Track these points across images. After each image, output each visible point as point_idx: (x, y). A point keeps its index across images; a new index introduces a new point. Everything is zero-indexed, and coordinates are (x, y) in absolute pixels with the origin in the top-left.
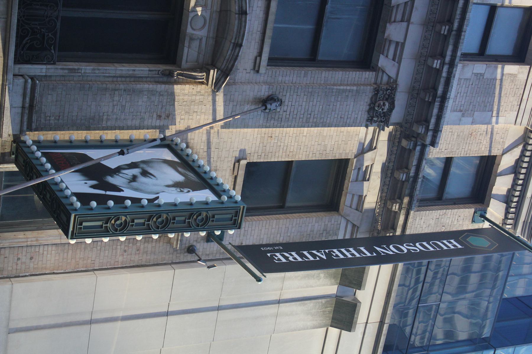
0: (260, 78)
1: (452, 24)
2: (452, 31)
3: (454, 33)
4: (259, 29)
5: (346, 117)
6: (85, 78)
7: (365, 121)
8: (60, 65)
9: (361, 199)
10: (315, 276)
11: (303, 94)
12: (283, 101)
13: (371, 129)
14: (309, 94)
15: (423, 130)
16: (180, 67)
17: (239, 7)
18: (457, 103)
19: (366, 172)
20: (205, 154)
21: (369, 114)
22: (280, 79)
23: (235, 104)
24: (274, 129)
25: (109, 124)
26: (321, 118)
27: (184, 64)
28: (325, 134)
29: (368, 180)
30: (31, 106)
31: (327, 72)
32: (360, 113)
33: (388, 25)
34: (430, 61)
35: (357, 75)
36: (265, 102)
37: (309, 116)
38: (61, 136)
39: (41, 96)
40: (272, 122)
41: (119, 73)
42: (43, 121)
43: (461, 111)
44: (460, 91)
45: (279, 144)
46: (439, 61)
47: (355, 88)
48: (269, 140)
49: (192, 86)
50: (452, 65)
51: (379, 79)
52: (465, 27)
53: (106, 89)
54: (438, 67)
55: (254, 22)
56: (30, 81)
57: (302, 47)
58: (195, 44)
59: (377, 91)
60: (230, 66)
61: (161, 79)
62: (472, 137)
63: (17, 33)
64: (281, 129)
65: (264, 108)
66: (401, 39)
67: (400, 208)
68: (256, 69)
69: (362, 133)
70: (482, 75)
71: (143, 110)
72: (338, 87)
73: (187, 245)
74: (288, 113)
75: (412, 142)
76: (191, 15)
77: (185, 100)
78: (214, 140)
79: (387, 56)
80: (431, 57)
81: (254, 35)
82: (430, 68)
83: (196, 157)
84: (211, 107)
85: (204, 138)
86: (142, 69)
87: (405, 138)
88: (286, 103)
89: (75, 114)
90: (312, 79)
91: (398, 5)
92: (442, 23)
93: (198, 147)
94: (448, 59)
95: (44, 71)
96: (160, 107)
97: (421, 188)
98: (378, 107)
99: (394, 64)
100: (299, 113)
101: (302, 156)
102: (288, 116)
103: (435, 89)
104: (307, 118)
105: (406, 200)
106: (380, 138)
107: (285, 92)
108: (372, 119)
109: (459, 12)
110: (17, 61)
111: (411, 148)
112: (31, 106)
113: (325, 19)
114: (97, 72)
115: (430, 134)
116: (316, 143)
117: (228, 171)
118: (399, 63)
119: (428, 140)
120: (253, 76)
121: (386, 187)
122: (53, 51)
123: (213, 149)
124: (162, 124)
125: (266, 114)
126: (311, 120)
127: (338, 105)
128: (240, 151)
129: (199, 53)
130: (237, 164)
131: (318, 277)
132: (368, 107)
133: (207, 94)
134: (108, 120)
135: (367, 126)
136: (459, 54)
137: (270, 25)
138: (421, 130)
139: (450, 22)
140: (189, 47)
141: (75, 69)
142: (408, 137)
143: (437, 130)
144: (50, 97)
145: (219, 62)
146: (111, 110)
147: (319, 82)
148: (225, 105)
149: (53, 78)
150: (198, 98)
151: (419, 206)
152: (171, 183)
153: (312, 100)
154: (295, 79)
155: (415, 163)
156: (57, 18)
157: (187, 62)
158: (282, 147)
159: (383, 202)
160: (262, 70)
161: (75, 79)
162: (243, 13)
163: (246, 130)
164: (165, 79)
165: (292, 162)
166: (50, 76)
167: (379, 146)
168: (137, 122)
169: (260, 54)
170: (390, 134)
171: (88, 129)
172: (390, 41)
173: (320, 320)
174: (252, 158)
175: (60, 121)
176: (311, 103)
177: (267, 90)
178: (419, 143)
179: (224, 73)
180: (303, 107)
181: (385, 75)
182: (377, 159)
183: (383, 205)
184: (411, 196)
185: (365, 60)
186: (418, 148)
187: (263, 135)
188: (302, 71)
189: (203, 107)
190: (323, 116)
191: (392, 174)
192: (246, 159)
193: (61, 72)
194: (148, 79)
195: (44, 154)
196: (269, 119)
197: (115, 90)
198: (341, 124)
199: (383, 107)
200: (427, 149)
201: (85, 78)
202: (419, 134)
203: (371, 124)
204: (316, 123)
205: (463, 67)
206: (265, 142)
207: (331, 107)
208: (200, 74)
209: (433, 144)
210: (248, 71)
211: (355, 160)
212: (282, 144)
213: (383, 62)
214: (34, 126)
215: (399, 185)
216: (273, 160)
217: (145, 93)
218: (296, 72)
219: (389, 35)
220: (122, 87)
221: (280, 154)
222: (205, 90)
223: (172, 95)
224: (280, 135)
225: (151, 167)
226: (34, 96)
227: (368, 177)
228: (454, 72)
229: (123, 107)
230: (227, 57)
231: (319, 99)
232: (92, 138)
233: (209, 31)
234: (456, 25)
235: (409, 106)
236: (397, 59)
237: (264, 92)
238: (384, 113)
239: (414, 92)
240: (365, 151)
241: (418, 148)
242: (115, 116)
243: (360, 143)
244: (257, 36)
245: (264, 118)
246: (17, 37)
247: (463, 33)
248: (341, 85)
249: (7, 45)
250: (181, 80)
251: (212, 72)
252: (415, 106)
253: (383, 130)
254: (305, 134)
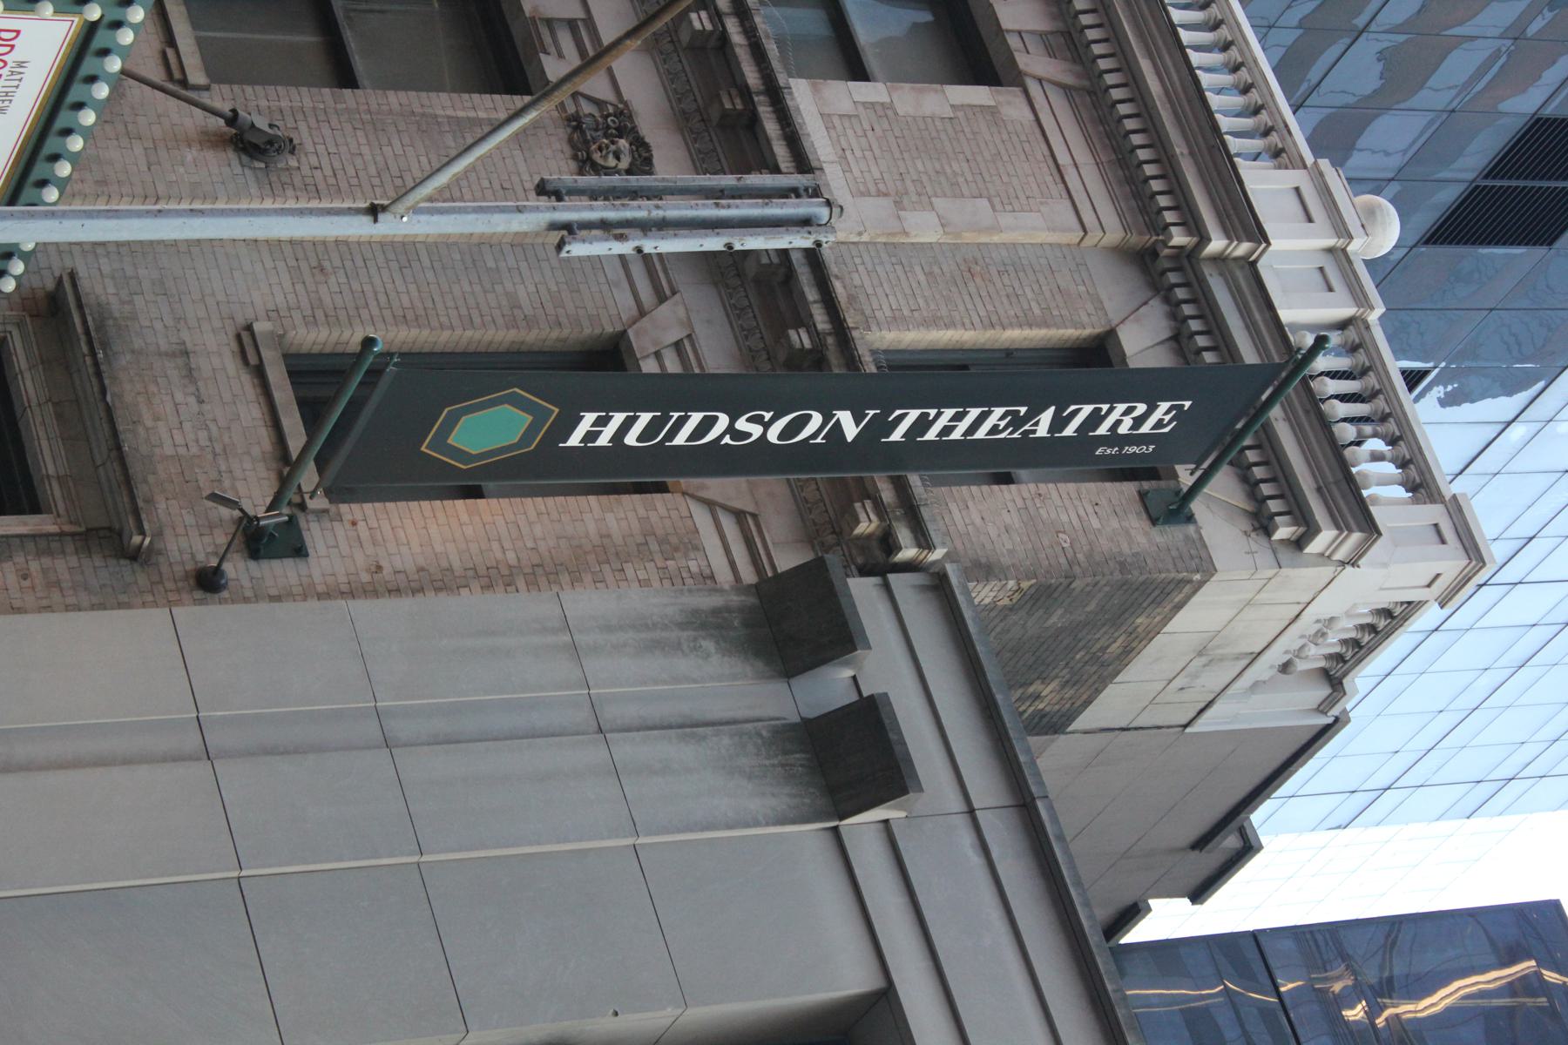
10: (685, 647)
11: (348, 128)
12: (296, 142)
18: (856, 172)
43: (886, 195)
44: (845, 146)
62: (978, 280)
70: (890, 106)
73: (190, 567)
74: (329, 172)
98: (600, 149)
100: (361, 174)
102: (332, 181)
125: (260, 174)
131: (695, 648)
153: (384, 141)
155: (811, 294)
158: (370, 295)
169: (171, 41)
172: (549, 22)
173: (790, 795)
180: (368, 157)
199: (613, 147)
219: (535, 9)
231: (406, 140)
252: (714, 150)
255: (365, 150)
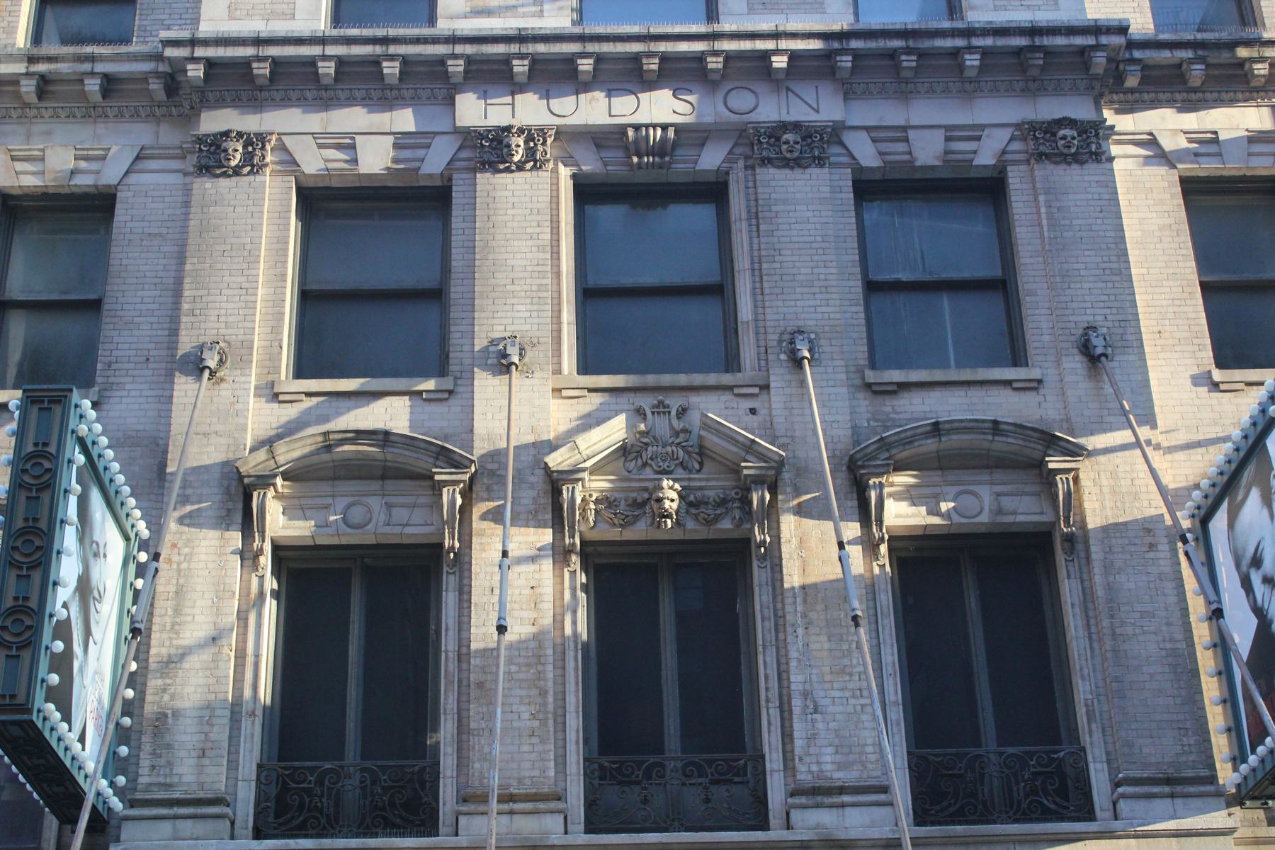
0: (1051, 374)
1: (895, 50)
2: (908, 47)
3: (911, 43)
4: (963, 393)
5: (1100, 203)
6: (1102, 691)
7: (1101, 166)
8: (1085, 739)
9: (1256, 138)
11: (1068, 292)
13: (1115, 150)
14: (1066, 279)
15: (1099, 54)
16: (1054, 524)
17: (927, 438)
19: (1200, 142)
20: (1211, 449)
21: (1086, 162)
22: (1047, 338)
23: (1105, 412)
24: (1143, 330)
25: (1179, 636)
26: (1108, 249)
27: (1047, 517)
28: (1139, 233)
29: (1216, 133)
30: (1168, 781)
31: (1021, 254)
32: (1086, 178)
33: (918, 163)
34: (968, 74)
35: (1018, 198)
36: (1093, 360)
37: (1107, 272)
38: (1216, 718)
39: (1146, 766)
40: (1129, 337)
41: (1082, 632)
42: (1192, 757)
45: (1171, 316)
46: (967, 57)
47: (1042, 198)
48: (1167, 335)
49: (1086, 497)
50: (969, 32)
51: (1017, 157)
52: (898, 27)
53: (1115, 651)
54: (978, 56)
55: (950, 406)
56: (1120, 790)
57: (986, 308)
58: (1007, 503)
59: (1041, 157)
60: (1036, 435)
61: (1082, 555)
63: (1038, 820)
64: (1141, 317)
65: (1103, 359)
66: (940, 134)
67: (1262, 59)
68: (1035, 385)
69: (1125, 163)
71: (1144, 578)
72: (1045, 229)
74: (1108, 311)
75: (1128, 68)
76: (957, 519)
77: (1112, 504)
78: (1182, 438)
79: (975, 152)
80: (961, 72)
81: (974, 400)
82: (982, 69)
83: (1213, 470)
84: (1119, 454)
85: (1180, 456)
86: (1069, 590)
87: (1123, 83)
88: (1090, 318)
89: (1171, 701)
90: (1037, 279)
91: (881, 153)
92: (897, 67)
93: (1201, 465)
94: (960, 42)
95: (1099, 766)
96: (1133, 548)
97: (1212, 31)
99: (988, 136)
101: (1188, 269)
102: (1114, 311)
103: (1018, 52)
104: (1112, 274)
105: (1242, 52)
106: (1131, 128)
107: (1069, 325)
108: (1096, 154)
109: (872, 44)
110: (1090, 816)
111: (1138, 68)
112: (1168, 781)
113: (927, 278)
114: (1086, 671)
115: (1104, 40)
116: (1158, 246)
117: (1238, 400)
118: (983, 127)
119: (1117, 40)
120: (1049, 390)
121: (1224, 96)
122: (1062, 754)
123: (1201, 437)
124: (1165, 540)
125: (1117, 351)
126: (1115, 266)
127: (1080, 222)
128: (1195, 385)
129: (1023, 494)
130: (1222, 387)
132: (1074, 166)
133: (1095, 467)
134: (1172, 640)
135: (1111, 159)
136: (947, 24)
137: (953, 375)
138: (1100, 59)
139: (892, 55)
140: (1015, 513)
141: (1088, 713)
142: (1120, 78)
143: (1096, 29)
144: (1145, 750)
145: (1032, 456)
146: (1153, 637)
147: (1042, 267)
148: (1111, 430)
149: (1111, 748)
150: (1105, 482)
151: (1256, 24)
152: (1265, 512)
153: (1076, 273)
154: (1043, 311)
155: (1166, 54)
156: (1001, 754)
157: (1042, 513)
158: (1176, 309)
159: (1255, 95)
160: (1035, 373)
161: (1106, 708)
162: (936, 429)
163: (1152, 382)
164: (1080, 547)
165: (1202, 284)
166: (1108, 753)
167: (1147, 128)
168: (1169, 586)
169: (1008, 383)
170: (1118, 112)
171: (1195, 673)
172: (946, 153)
174: (1206, 361)
175: (1188, 725)
176: (1082, 273)
177: (1071, 358)
178: (1127, 56)
179: (1051, 442)
180: (1091, 285)
181: (1008, 149)
182: (1171, 125)
183: (1262, 94)
184: (1232, 45)
185: (990, 190)
186: (1137, 54)
187: (1159, 348)
188: (1026, 300)
189: (1120, 469)
190: (1104, 246)
191: (1195, 90)
192: (1210, 372)
193: (1097, 735)
194: (1085, 577)
195: (1253, 751)
196: (1124, 344)
197: (1114, 634)
198: (1114, 209)
200: (1134, 37)
201: (1102, 691)
202: (1109, 60)
203: (1104, 153)
204: (1118, 256)
205: (972, 8)
206: (1171, 342)
207: (1084, 234)
208: (1060, 486)
209: (1122, 29)
210: (1041, 398)
211: (1179, 166)
212: (1170, 309)
213: (986, 156)
214: (1205, 773)
215: (1216, 72)
216: (1204, 321)
217: (1111, 579)
218: (1029, 312)
219: (937, 158)
220: (1106, 623)
221: (1191, 309)
222: (1086, 469)
223: (1108, 530)
224: (1154, 316)
225: (1244, 550)
226: (1148, 778)
227: (1209, 135)
228: (982, 25)
229: (1144, 615)
230: (1021, 442)
231: (1073, 260)
232: (1212, 663)
233: (980, 483)
234: (897, 43)
235: (1058, 91)
236: (975, 133)
237: (1075, 364)
238: (1079, 135)
239: (1033, 88)
240: (1159, 152)
241: (1137, 54)
242: (1164, 628)
243: (1146, 164)
244: (975, 394)
245: (1124, 354)
246: (1046, 820)
247: (909, 27)
248: (1040, 225)
249: (1059, 837)
250: (1078, 518)
251: (1051, 466)
253: (1112, 127)
254: (1145, 271)
255: (1086, 285)
